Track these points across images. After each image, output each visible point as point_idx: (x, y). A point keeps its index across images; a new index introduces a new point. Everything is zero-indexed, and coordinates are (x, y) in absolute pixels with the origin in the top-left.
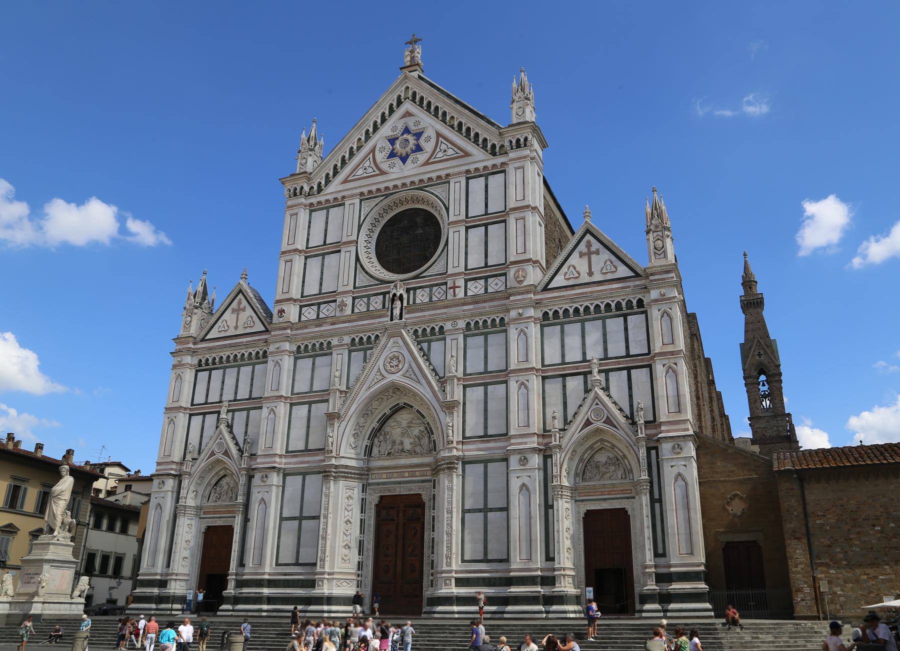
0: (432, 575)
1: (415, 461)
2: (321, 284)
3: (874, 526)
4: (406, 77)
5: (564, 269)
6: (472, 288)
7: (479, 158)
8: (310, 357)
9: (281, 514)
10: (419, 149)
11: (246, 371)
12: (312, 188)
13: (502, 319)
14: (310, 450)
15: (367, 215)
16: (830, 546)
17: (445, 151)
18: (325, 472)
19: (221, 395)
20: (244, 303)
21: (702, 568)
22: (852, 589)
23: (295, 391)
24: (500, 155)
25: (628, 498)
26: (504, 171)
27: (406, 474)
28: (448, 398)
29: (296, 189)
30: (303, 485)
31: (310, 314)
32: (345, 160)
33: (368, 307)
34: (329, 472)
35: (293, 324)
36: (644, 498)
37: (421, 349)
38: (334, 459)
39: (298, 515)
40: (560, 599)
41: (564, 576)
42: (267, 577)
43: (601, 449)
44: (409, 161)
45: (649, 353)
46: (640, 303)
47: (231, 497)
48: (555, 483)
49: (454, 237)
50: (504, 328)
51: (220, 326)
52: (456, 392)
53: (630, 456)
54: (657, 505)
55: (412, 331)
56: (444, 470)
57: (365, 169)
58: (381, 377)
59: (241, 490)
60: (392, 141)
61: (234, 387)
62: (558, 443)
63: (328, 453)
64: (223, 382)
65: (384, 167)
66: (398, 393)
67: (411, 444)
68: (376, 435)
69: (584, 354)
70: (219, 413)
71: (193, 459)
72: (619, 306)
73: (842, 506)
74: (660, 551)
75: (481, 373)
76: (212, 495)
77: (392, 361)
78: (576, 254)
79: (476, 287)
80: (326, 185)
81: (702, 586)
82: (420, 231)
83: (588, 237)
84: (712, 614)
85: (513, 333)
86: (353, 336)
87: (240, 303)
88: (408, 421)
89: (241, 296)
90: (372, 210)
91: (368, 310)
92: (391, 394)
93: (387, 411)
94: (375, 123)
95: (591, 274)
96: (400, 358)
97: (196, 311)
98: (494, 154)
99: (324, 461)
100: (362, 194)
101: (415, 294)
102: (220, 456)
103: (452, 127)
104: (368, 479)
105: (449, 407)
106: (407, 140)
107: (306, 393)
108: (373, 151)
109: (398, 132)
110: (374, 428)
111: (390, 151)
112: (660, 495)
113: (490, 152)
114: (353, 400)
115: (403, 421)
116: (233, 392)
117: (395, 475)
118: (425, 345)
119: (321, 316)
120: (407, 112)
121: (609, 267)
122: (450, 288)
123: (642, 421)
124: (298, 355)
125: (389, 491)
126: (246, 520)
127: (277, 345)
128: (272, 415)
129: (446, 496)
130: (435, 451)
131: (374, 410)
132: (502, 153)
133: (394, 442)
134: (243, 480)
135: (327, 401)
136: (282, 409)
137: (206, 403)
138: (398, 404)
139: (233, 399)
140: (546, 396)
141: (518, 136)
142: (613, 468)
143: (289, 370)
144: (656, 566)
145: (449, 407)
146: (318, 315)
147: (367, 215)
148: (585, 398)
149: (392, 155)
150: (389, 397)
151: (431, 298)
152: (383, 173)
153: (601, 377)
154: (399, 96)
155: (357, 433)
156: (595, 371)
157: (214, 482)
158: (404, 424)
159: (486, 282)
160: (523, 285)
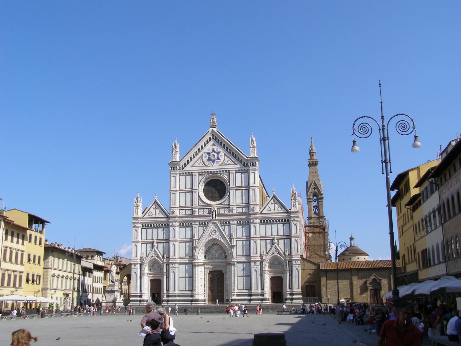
0: (227, 293)
1: (220, 261)
2: (186, 203)
3: (341, 283)
4: (213, 130)
5: (267, 207)
6: (238, 210)
7: (238, 166)
8: (185, 227)
9: (179, 276)
12: (180, 167)
13: (248, 221)
15: (201, 180)
16: (331, 287)
17: (228, 161)
19: (152, 237)
20: (157, 206)
21: (301, 292)
22: (335, 297)
23: (180, 238)
24: (247, 166)
25: (282, 274)
26: (248, 172)
28: (232, 244)
29: (174, 168)
31: (183, 213)
32: (191, 159)
33: (203, 213)
35: (178, 216)
36: (287, 274)
37: (222, 228)
39: (184, 276)
40: (265, 299)
41: (266, 294)
42: (177, 294)
43: (275, 260)
44: (216, 162)
45: (290, 235)
46: (288, 220)
47: (159, 270)
48: (263, 270)
49: (232, 193)
50: (248, 224)
51: (149, 214)
52: (234, 243)
53: (284, 263)
54: (290, 276)
55: (219, 222)
57: (199, 163)
59: (165, 269)
60: (209, 154)
61: (157, 235)
62: (264, 259)
63: (194, 258)
64: (152, 233)
65: (207, 164)
67: (218, 255)
69: (272, 234)
70: (152, 243)
71: (145, 258)
72: (282, 221)
73: (335, 278)
74: (291, 288)
75: (242, 237)
76: (151, 269)
78: (270, 203)
79: (239, 210)
80: (185, 167)
81: (301, 296)
82: (219, 187)
83: (274, 198)
84: (303, 303)
85: (252, 226)
89: (155, 203)
90: (202, 179)
91: (203, 214)
92: (212, 241)
93: (210, 245)
94: (202, 146)
95: (275, 210)
96: (216, 231)
97: (139, 207)
98: (245, 166)
99: (193, 260)
100: (199, 172)
101: (219, 210)
103: (230, 153)
105: (233, 247)
106: (214, 155)
108: (202, 156)
109: (211, 151)
111: (208, 158)
112: (291, 273)
113: (243, 165)
116: (157, 237)
117: (214, 265)
118: (223, 227)
119: (187, 214)
121: (280, 209)
122: (232, 210)
123: (288, 254)
124: (180, 226)
126: (168, 278)
127: (174, 223)
128: (173, 246)
129: (233, 272)
130: (227, 258)
132: (247, 166)
133: (213, 255)
134: (165, 265)
136: (177, 244)
137: (147, 240)
138: (214, 244)
139: (157, 239)
140: (261, 245)
141: (253, 162)
142: (279, 266)
144: (290, 292)
145: (233, 247)
146: (186, 213)
147: (201, 180)
148: (272, 247)
149: (209, 159)
151: (225, 212)
152: (206, 166)
153: (276, 241)
154: (210, 137)
156: (275, 239)
157: (152, 265)
158: (216, 249)
159: (242, 209)
160: (254, 212)
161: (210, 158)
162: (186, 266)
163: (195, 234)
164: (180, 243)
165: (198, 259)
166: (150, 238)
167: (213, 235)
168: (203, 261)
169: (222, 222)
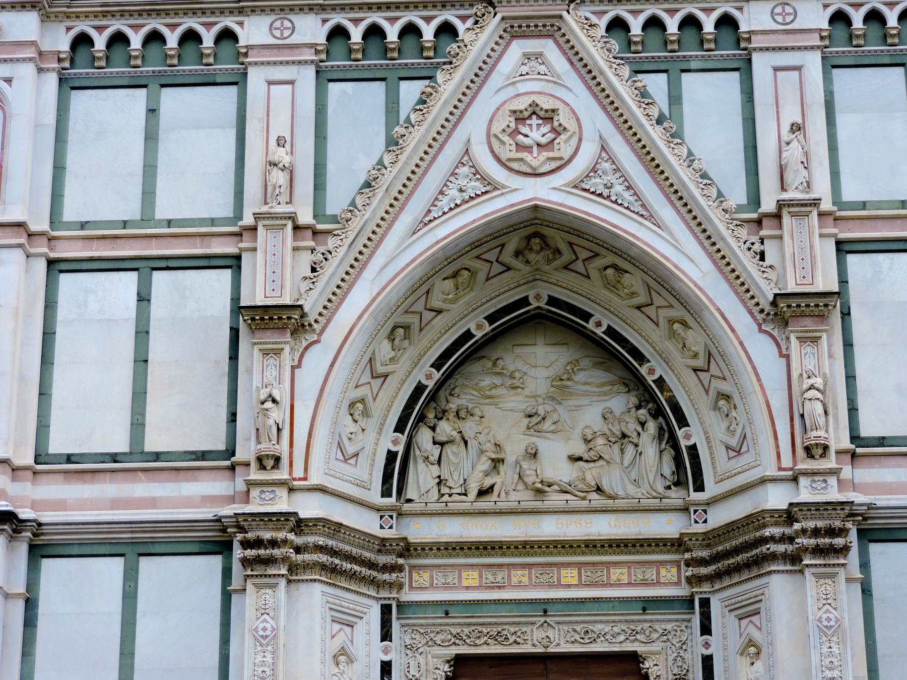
14: (157, 456)
18: (258, 543)
27: (569, 576)
30: (130, 597)
34: (273, 543)
38: (283, 492)
55: (603, 22)
56: (794, 559)
58: (476, 186)
63: (263, 467)
66: (532, 257)
68: (421, 418)
77: (525, 130)
86: (337, 19)
88: (551, 372)
92: (507, 257)
96: (563, 118)
104: (400, 587)
107: (125, 224)
110: (419, 389)
114: (358, 265)
115: (532, 372)
117: (518, 575)
118: (657, 84)
125: (497, 638)
129: (815, 659)
130: (700, 487)
131: (428, 315)
135: (234, 263)
138: (524, 301)
143: (37, 126)
150: (497, 268)
155: (362, 401)
162: (131, 577)
163: (282, 155)
164: (66, 281)
165: (315, 479)
167: (535, 174)
168: (368, 523)
169: (636, 26)
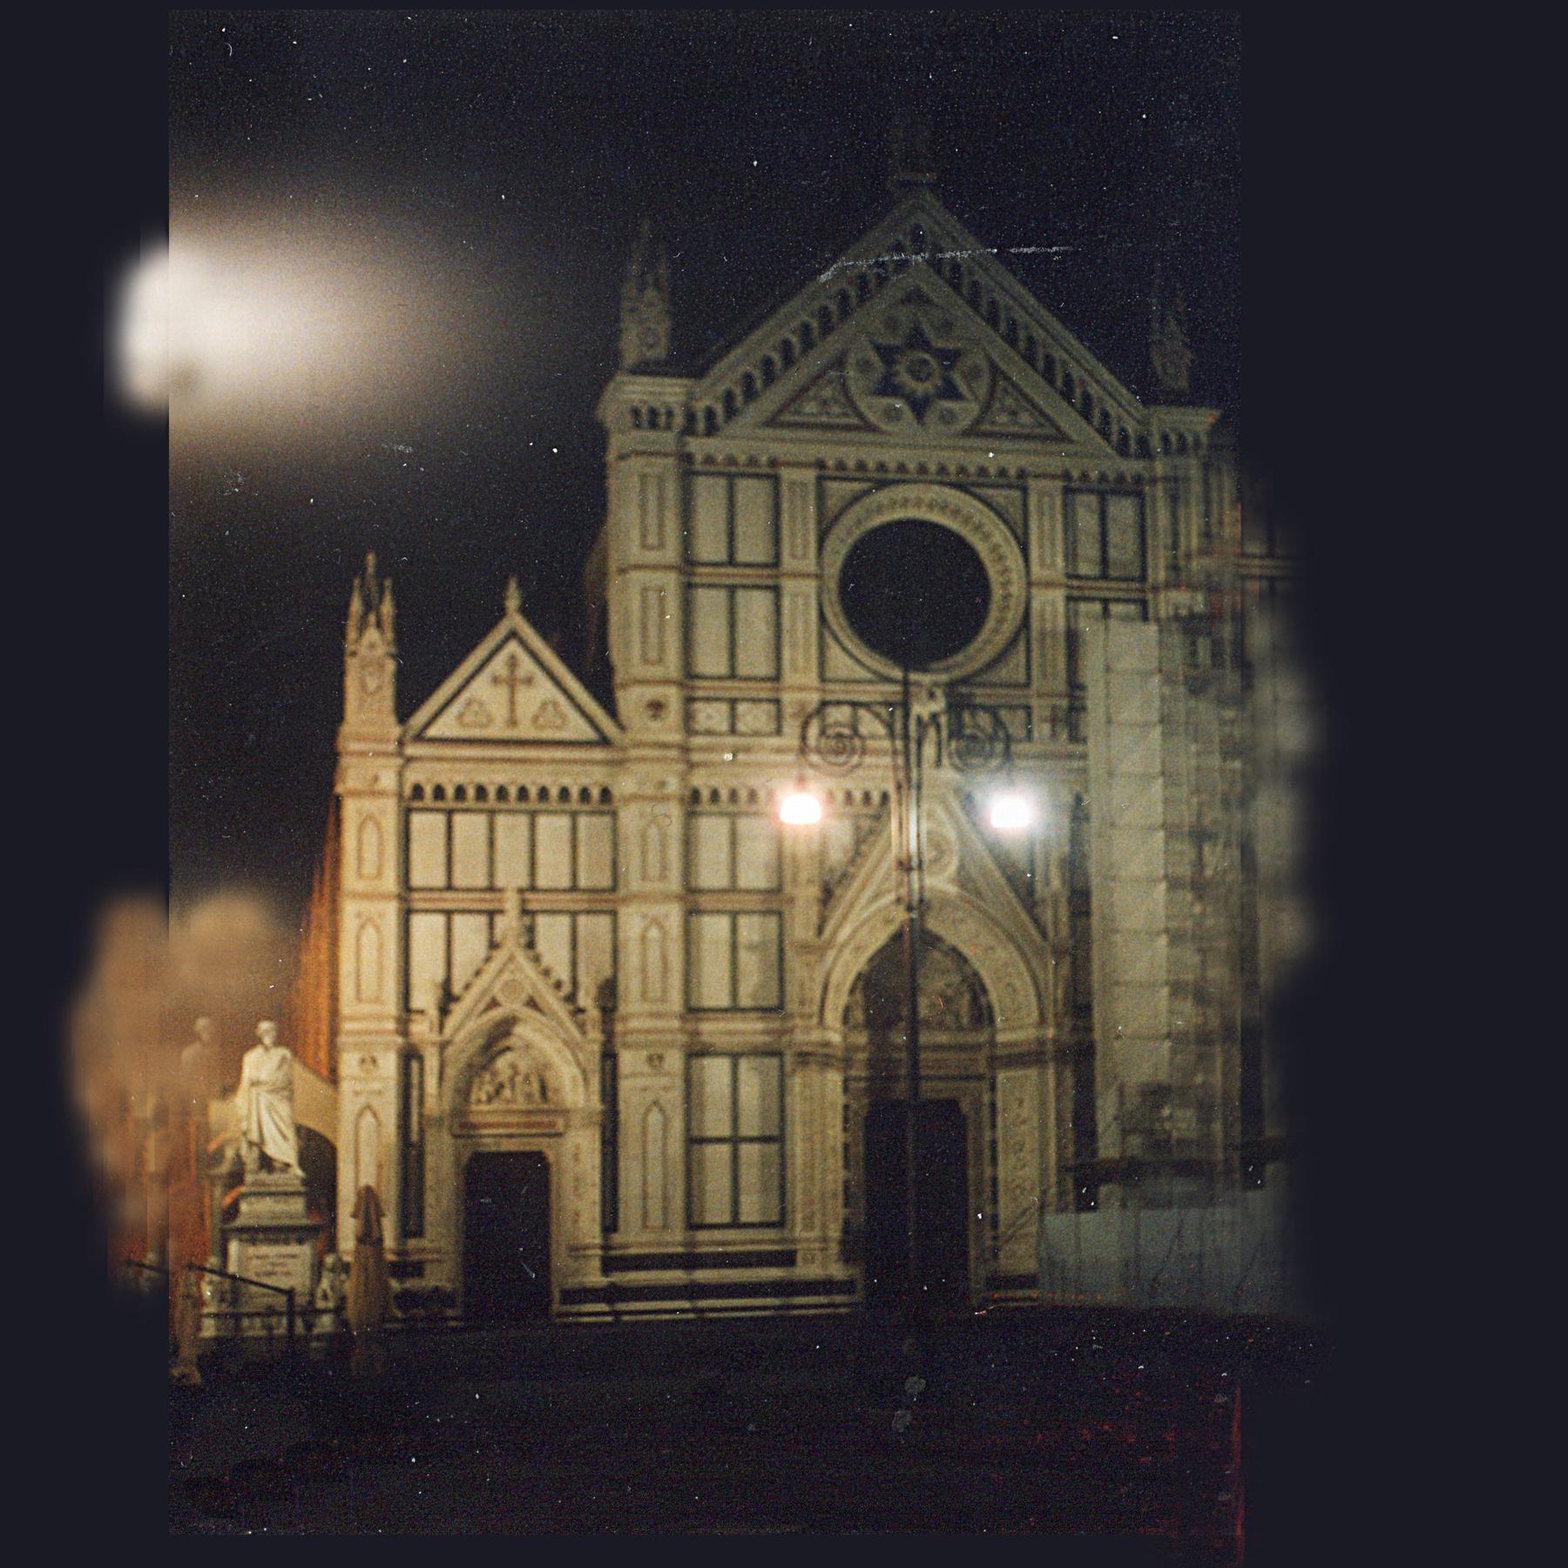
10: (951, 392)
11: (553, 827)
12: (691, 417)
19: (491, 874)
64: (491, 843)
70: (491, 914)
87: (513, 663)
98: (1122, 450)
100: (821, 465)
102: (510, 1006)
103: (1030, 359)
106: (925, 362)
116: (522, 868)
120: (918, 290)
139: (523, 882)
149: (888, 387)
161: (897, 380)
166: (470, 873)
